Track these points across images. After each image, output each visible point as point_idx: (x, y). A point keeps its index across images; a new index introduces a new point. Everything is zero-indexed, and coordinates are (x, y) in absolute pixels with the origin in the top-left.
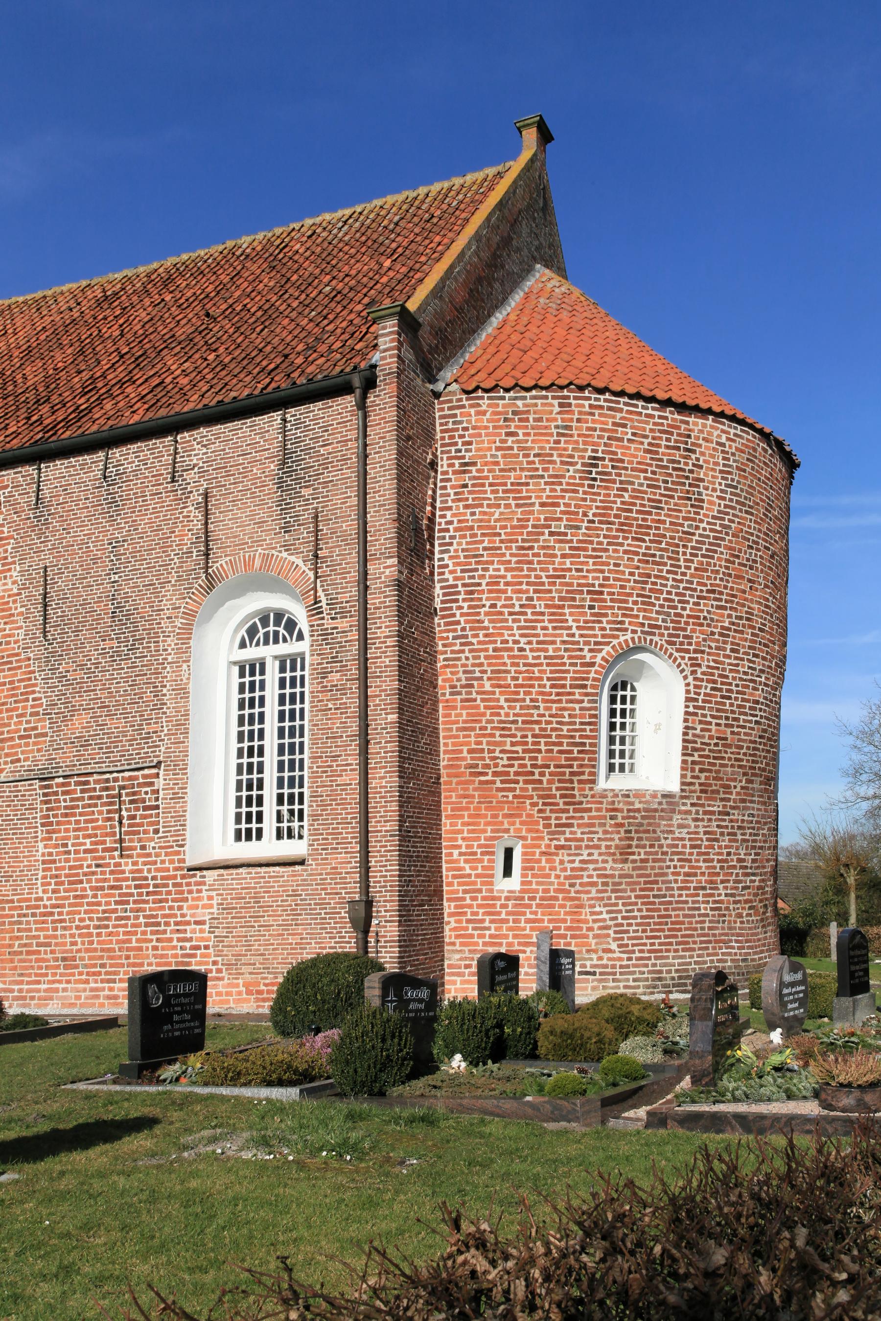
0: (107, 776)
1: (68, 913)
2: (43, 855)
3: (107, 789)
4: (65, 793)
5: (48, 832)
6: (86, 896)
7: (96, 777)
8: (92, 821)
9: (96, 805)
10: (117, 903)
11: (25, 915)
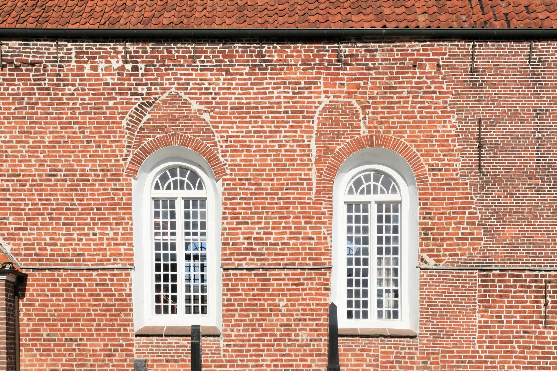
0: (537, 273)
1: (499, 363)
2: (480, 322)
3: (536, 281)
4: (499, 281)
5: (485, 307)
6: (516, 352)
7: (527, 273)
8: (522, 302)
9: (526, 292)
10: (538, 358)
11: (462, 362)
